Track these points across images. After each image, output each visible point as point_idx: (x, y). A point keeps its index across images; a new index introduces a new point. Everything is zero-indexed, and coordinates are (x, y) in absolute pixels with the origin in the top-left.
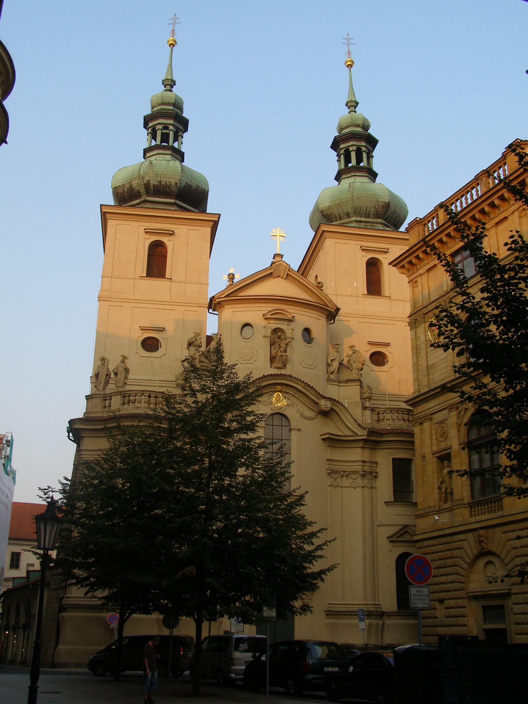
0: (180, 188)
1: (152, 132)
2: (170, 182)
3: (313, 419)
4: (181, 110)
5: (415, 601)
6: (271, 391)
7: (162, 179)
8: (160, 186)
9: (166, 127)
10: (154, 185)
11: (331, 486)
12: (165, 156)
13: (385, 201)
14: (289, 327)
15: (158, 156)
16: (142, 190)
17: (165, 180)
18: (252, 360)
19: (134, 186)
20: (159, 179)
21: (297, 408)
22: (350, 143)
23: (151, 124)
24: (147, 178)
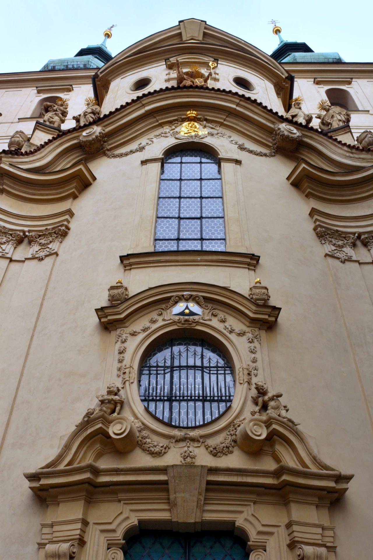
6: (176, 120)
7: (69, 63)
11: (332, 256)
13: (335, 57)
17: (72, 63)
20: (66, 64)
21: (232, 139)
24: (52, 65)
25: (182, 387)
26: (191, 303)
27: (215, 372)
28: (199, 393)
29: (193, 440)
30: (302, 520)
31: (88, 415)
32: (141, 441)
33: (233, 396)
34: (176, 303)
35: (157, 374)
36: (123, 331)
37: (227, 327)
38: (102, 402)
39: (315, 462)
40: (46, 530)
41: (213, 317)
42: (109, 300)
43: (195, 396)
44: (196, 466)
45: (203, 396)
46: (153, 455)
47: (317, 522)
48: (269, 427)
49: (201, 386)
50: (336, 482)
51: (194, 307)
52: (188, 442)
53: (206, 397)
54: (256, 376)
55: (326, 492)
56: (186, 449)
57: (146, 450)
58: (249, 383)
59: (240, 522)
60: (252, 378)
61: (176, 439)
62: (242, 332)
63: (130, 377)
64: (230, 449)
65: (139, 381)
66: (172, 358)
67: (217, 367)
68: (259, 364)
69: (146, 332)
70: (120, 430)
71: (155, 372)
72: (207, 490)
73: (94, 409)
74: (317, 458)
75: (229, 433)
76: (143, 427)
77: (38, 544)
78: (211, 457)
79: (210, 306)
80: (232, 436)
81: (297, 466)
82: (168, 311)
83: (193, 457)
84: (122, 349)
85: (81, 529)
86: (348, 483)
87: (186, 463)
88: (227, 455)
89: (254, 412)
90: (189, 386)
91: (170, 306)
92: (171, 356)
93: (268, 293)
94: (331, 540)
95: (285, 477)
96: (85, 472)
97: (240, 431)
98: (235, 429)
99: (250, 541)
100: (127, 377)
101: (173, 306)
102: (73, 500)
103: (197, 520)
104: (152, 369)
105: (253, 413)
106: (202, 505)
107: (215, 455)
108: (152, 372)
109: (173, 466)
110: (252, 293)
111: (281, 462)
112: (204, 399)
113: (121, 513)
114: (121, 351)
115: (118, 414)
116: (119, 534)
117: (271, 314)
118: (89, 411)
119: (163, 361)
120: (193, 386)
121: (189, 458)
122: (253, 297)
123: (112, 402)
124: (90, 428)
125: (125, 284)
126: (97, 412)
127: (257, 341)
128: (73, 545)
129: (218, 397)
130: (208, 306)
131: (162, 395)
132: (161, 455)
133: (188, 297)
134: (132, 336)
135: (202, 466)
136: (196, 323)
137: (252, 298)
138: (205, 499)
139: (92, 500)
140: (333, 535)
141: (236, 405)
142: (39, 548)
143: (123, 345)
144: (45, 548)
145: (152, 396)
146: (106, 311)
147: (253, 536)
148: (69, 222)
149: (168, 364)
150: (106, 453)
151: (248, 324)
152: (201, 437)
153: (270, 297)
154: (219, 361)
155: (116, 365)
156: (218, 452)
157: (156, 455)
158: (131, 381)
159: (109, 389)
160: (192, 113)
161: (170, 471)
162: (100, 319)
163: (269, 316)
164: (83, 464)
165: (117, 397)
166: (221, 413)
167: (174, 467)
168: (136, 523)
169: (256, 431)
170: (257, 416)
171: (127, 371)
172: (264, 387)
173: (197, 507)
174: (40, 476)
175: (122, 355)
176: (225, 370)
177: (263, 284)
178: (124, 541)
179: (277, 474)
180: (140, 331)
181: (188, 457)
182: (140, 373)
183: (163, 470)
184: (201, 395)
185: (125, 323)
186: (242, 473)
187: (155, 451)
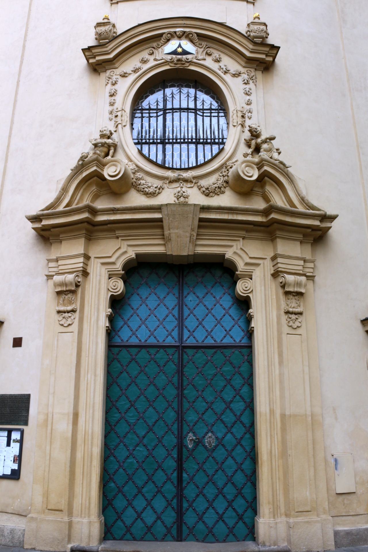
25: (175, 129)
26: (184, 41)
27: (209, 114)
28: (192, 136)
29: (186, 181)
30: (287, 254)
31: (82, 158)
32: (135, 182)
33: (226, 139)
34: (168, 40)
35: (150, 117)
36: (113, 72)
37: (222, 67)
38: (96, 145)
39: (302, 202)
40: (52, 264)
41: (207, 56)
42: (96, 39)
43: (188, 139)
44: (189, 204)
45: (196, 139)
46: (148, 196)
47: (299, 255)
48: (261, 168)
49: (194, 129)
50: (321, 221)
51: (187, 46)
52: (181, 183)
53: (199, 139)
54: (250, 119)
55: (310, 230)
56: (179, 189)
57: (141, 191)
58: (243, 126)
59: (229, 254)
60: (246, 121)
61: (169, 180)
62: (237, 73)
63: (122, 120)
64: (222, 189)
65: (132, 124)
66: (165, 101)
67: (211, 109)
68: (253, 107)
69: (137, 73)
70: (115, 172)
71: (147, 115)
72: (199, 227)
73: (88, 153)
74: (305, 199)
75: (221, 175)
76: (137, 169)
77: (47, 276)
78: (203, 197)
79: (204, 44)
80: (224, 177)
81: (286, 205)
82: (160, 50)
83: (186, 197)
84: (113, 92)
85: (83, 262)
86: (331, 222)
87: (179, 202)
88: (218, 195)
89: (247, 154)
90: (182, 129)
91: (162, 44)
92: (164, 98)
93: (267, 29)
94: (311, 270)
95: (273, 216)
96: (83, 212)
97: (232, 173)
98: (228, 170)
99: (238, 271)
100: (119, 119)
101: (164, 44)
102: (75, 238)
103: (190, 253)
104: (144, 111)
105: (245, 155)
106: (195, 240)
107: (207, 195)
108: (144, 115)
109: (167, 205)
110: (250, 30)
111: (270, 201)
112: (197, 142)
113: (120, 248)
114: (112, 94)
115: (112, 157)
116: (119, 266)
117: (268, 53)
118: (83, 155)
119: (156, 104)
120: (186, 129)
121: (182, 197)
122: (250, 34)
123: (106, 145)
124: (85, 171)
125: (112, 21)
126: (91, 155)
127: (253, 82)
128: (77, 276)
129: (211, 139)
130: (202, 44)
131: (155, 137)
132: (156, 195)
133: (181, 34)
134: (122, 78)
135: (195, 204)
136: (189, 63)
137: (249, 36)
138: (198, 235)
139: (92, 238)
140: (313, 267)
141: (229, 147)
142: (48, 279)
143: (114, 87)
144: (53, 279)
145: (145, 139)
146: (94, 51)
147: (241, 266)
149: (161, 106)
150: (102, 195)
151: (243, 63)
152: (194, 178)
153: (268, 35)
154: (212, 103)
156: (210, 193)
157: (150, 195)
158: (124, 124)
159: (102, 132)
161: (164, 209)
162: (88, 60)
163: (267, 55)
164: (80, 205)
165: (109, 141)
166: (213, 155)
167: (168, 206)
168: (134, 256)
169: (247, 172)
170: (249, 158)
171: (119, 114)
172: (258, 130)
173: (190, 242)
174: (41, 217)
175: (113, 98)
176: (218, 113)
177: (262, 20)
178: (123, 272)
179: (266, 212)
180: (131, 72)
181: (181, 196)
182: (133, 117)
183: (158, 209)
184: (194, 137)
185: (114, 64)
186: (232, 211)
187: (149, 192)
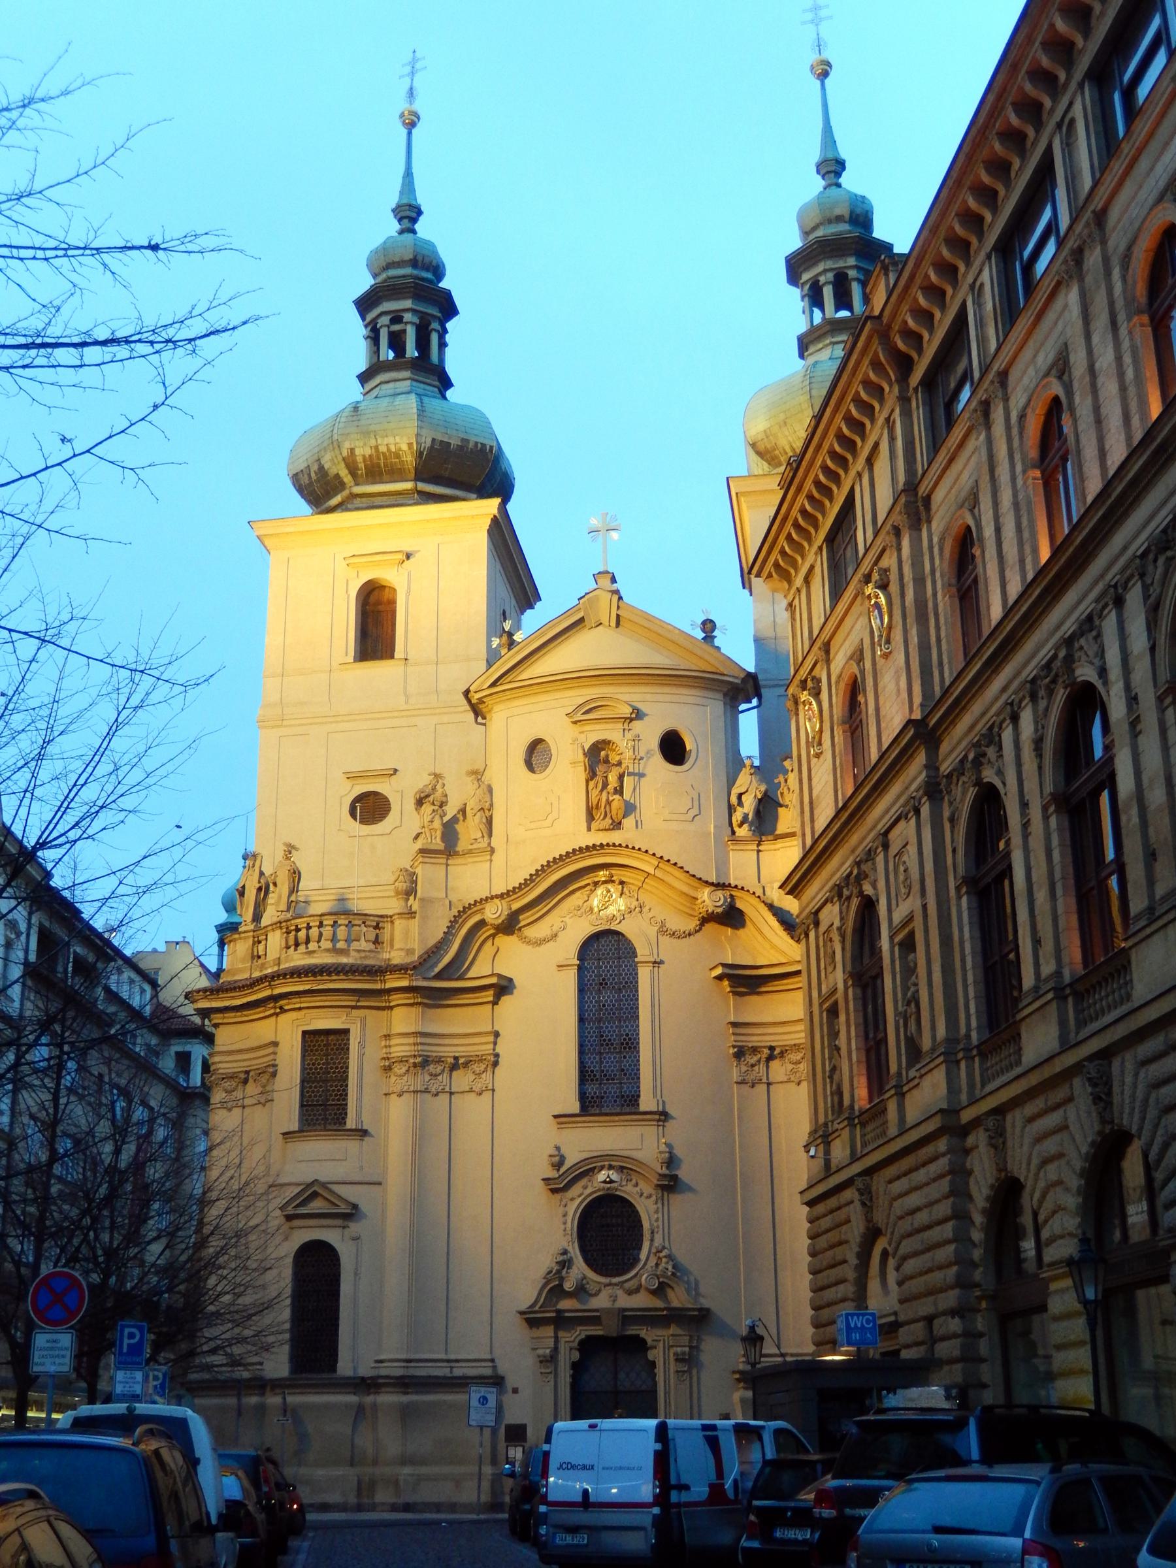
0: (421, 453)
1: (372, 335)
2: (395, 444)
3: (690, 935)
4: (438, 271)
5: (43, 1360)
6: (588, 884)
8: (379, 458)
9: (397, 318)
10: (364, 456)
11: (742, 1082)
12: (398, 384)
14: (629, 735)
15: (384, 387)
16: (344, 473)
18: (550, 819)
19: (326, 467)
20: (373, 442)
22: (820, 268)
23: (369, 317)
24: (347, 445)
29: (616, 1284)
51: (614, 1176)
116: (576, 1344)
148: (495, 1043)
155: (563, 1227)
160: (602, 875)
